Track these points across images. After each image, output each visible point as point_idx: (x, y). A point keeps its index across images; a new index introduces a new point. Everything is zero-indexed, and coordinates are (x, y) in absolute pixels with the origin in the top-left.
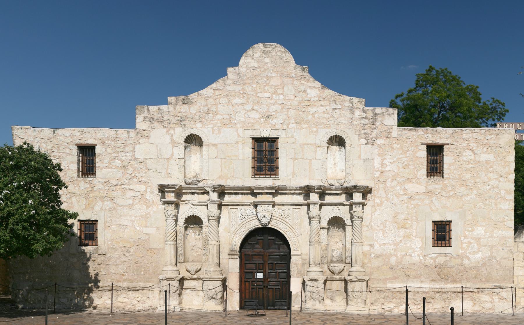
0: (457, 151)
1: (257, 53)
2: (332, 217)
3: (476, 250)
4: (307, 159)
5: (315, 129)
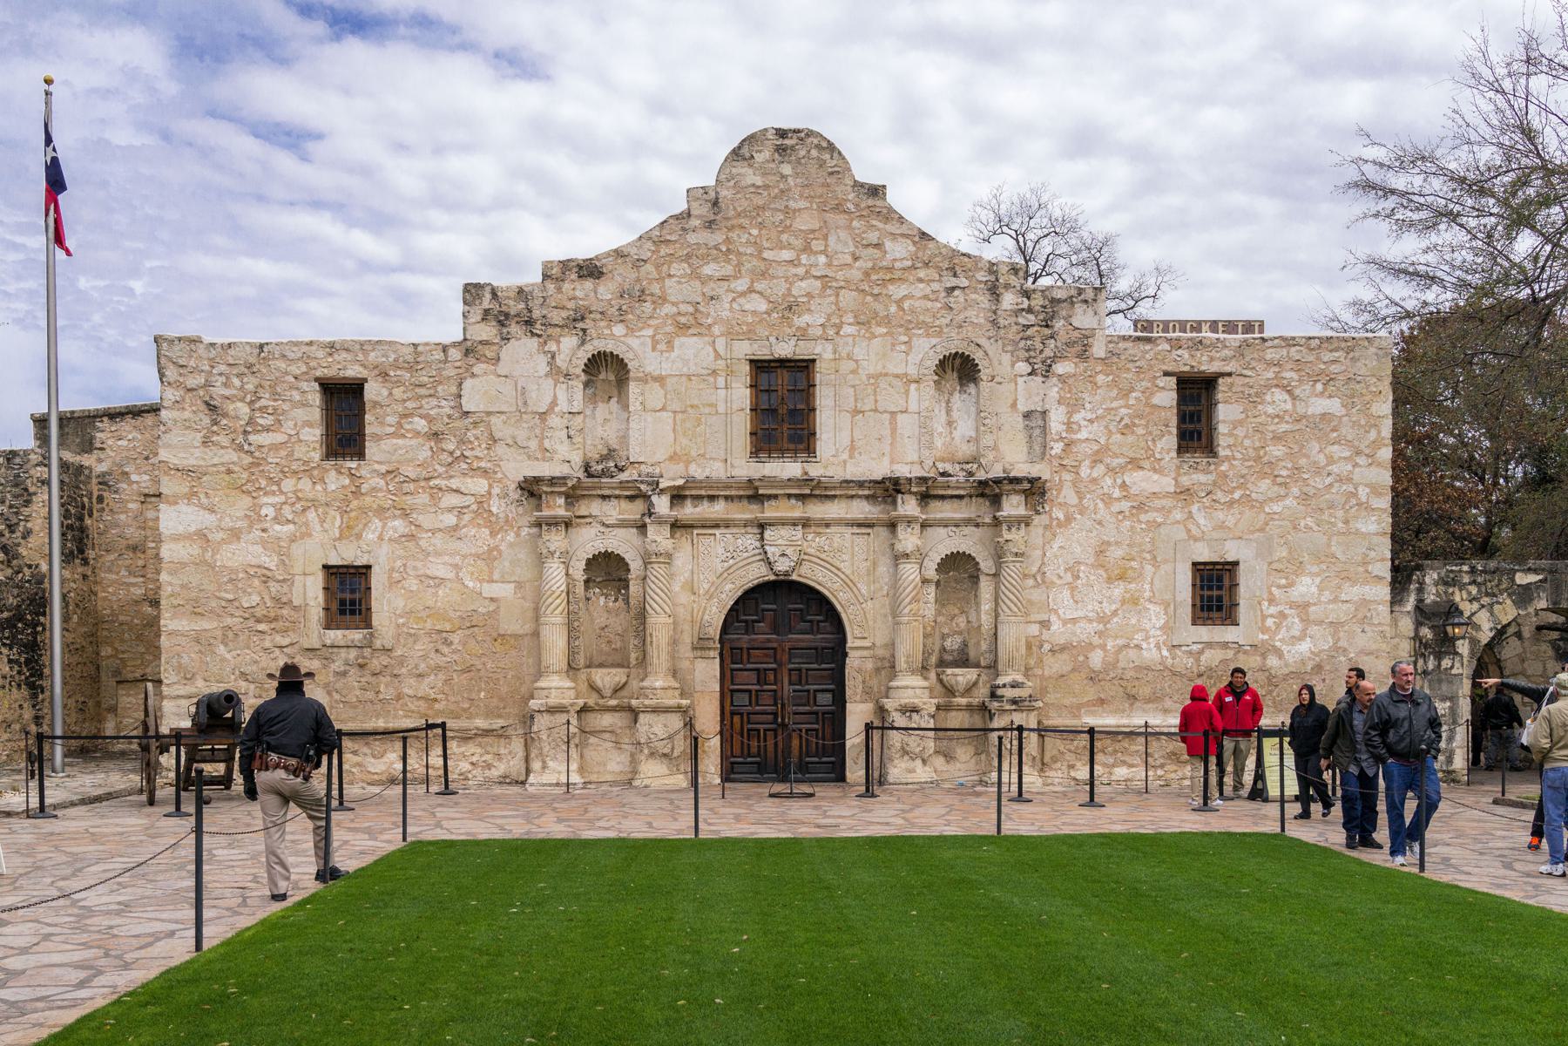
0: (1252, 391)
1: (760, 151)
3: (1297, 633)
4: (885, 412)
5: (905, 339)
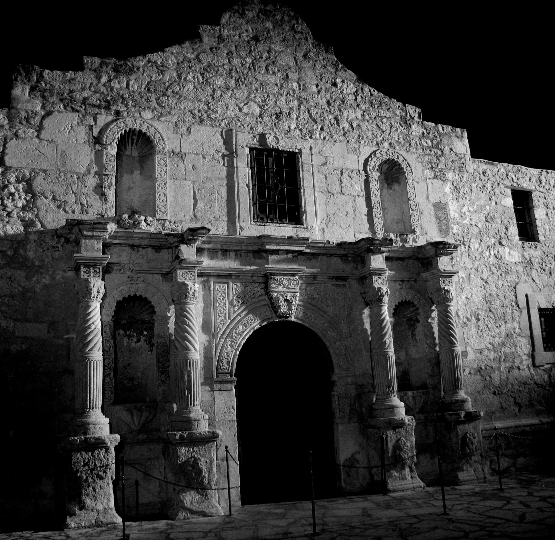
2: (400, 301)
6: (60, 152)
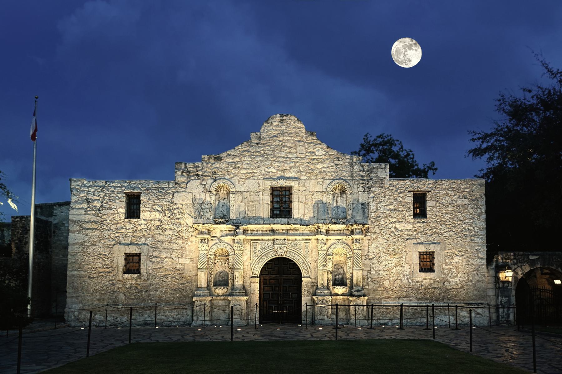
6: (193, 195)
